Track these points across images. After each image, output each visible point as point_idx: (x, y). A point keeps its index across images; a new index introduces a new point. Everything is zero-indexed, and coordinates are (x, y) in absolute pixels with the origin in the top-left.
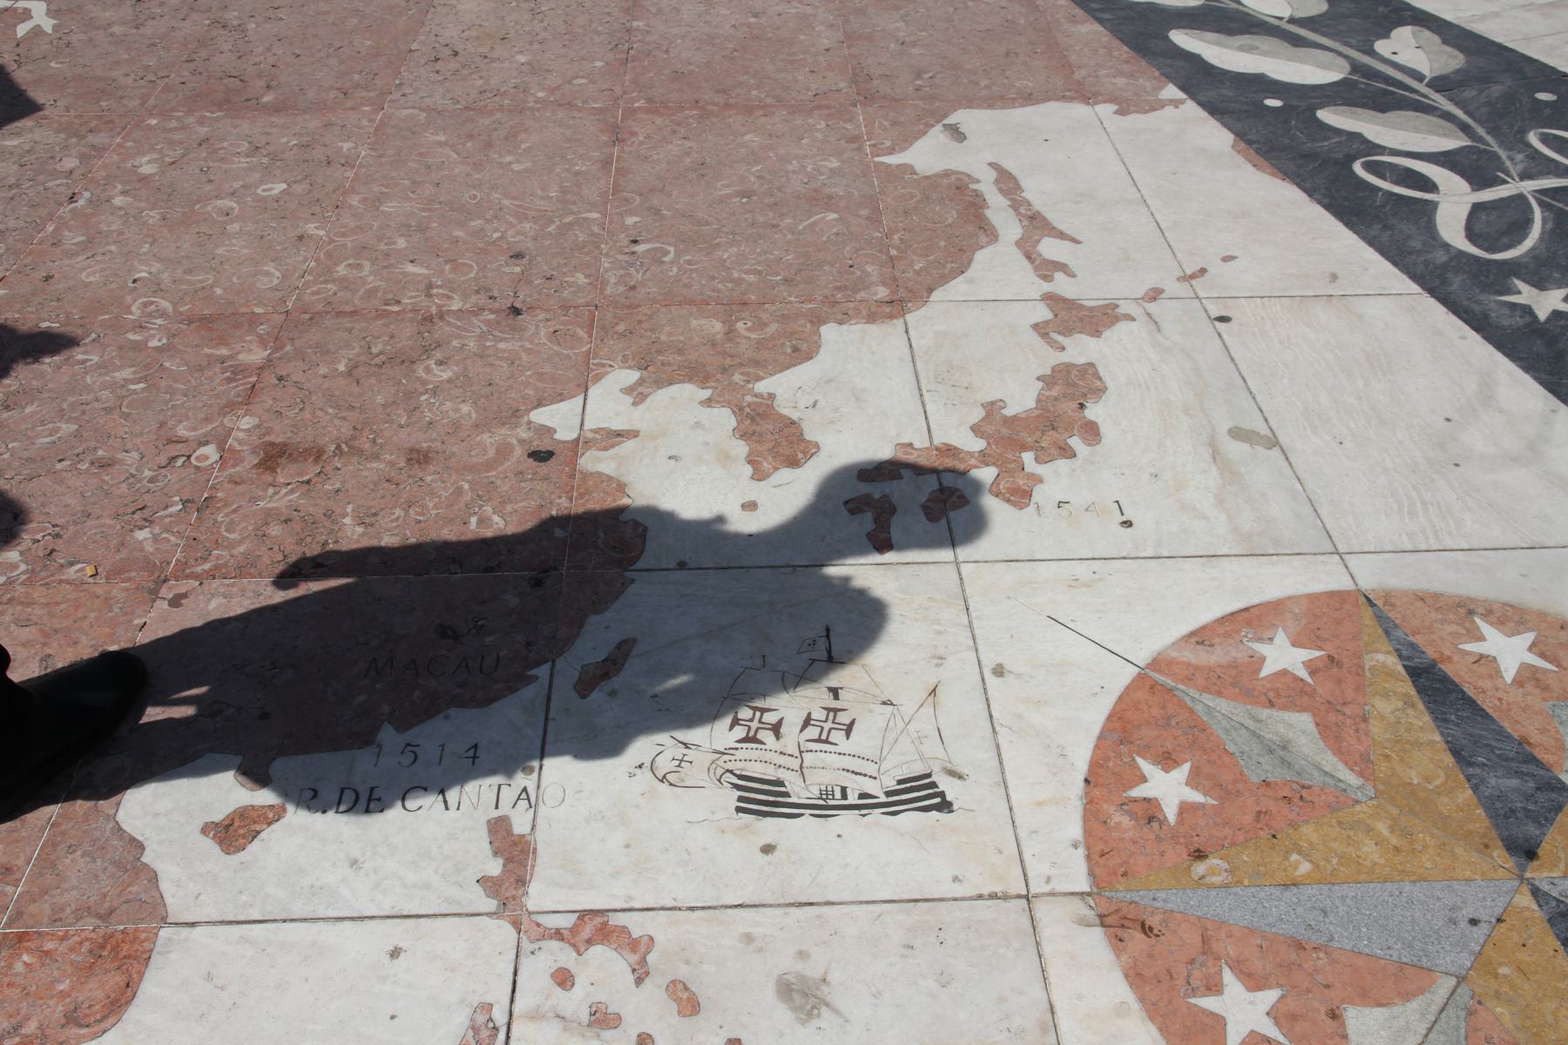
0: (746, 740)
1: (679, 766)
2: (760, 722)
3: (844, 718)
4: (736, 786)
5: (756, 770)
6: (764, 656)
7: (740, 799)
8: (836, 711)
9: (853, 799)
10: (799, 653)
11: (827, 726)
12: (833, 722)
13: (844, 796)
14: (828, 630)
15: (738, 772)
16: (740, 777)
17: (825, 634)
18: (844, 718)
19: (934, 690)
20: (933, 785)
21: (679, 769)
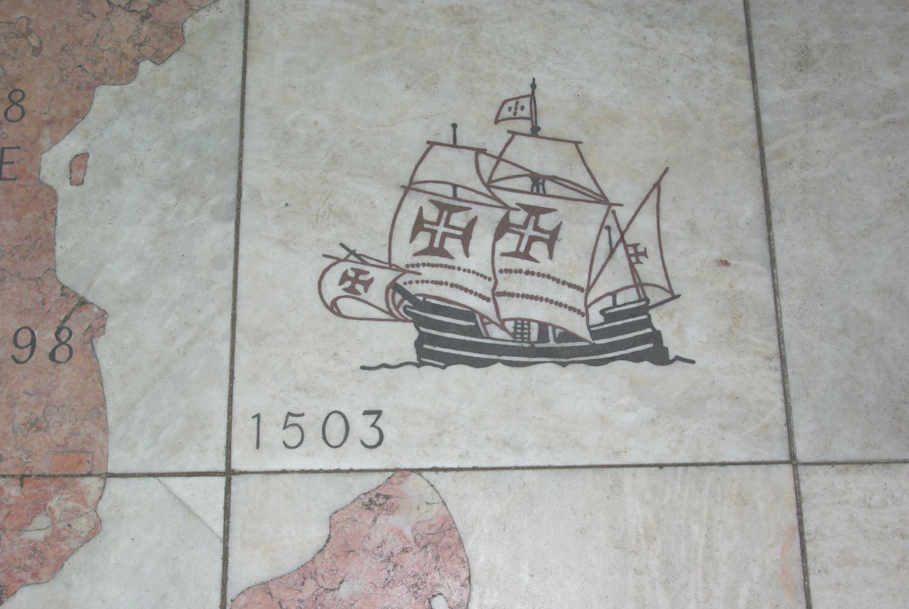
0: (430, 251)
3: (547, 222)
4: (418, 322)
6: (454, 126)
9: (552, 343)
10: (497, 121)
14: (533, 86)
15: (421, 298)
17: (529, 92)
19: (657, 185)
20: (648, 323)
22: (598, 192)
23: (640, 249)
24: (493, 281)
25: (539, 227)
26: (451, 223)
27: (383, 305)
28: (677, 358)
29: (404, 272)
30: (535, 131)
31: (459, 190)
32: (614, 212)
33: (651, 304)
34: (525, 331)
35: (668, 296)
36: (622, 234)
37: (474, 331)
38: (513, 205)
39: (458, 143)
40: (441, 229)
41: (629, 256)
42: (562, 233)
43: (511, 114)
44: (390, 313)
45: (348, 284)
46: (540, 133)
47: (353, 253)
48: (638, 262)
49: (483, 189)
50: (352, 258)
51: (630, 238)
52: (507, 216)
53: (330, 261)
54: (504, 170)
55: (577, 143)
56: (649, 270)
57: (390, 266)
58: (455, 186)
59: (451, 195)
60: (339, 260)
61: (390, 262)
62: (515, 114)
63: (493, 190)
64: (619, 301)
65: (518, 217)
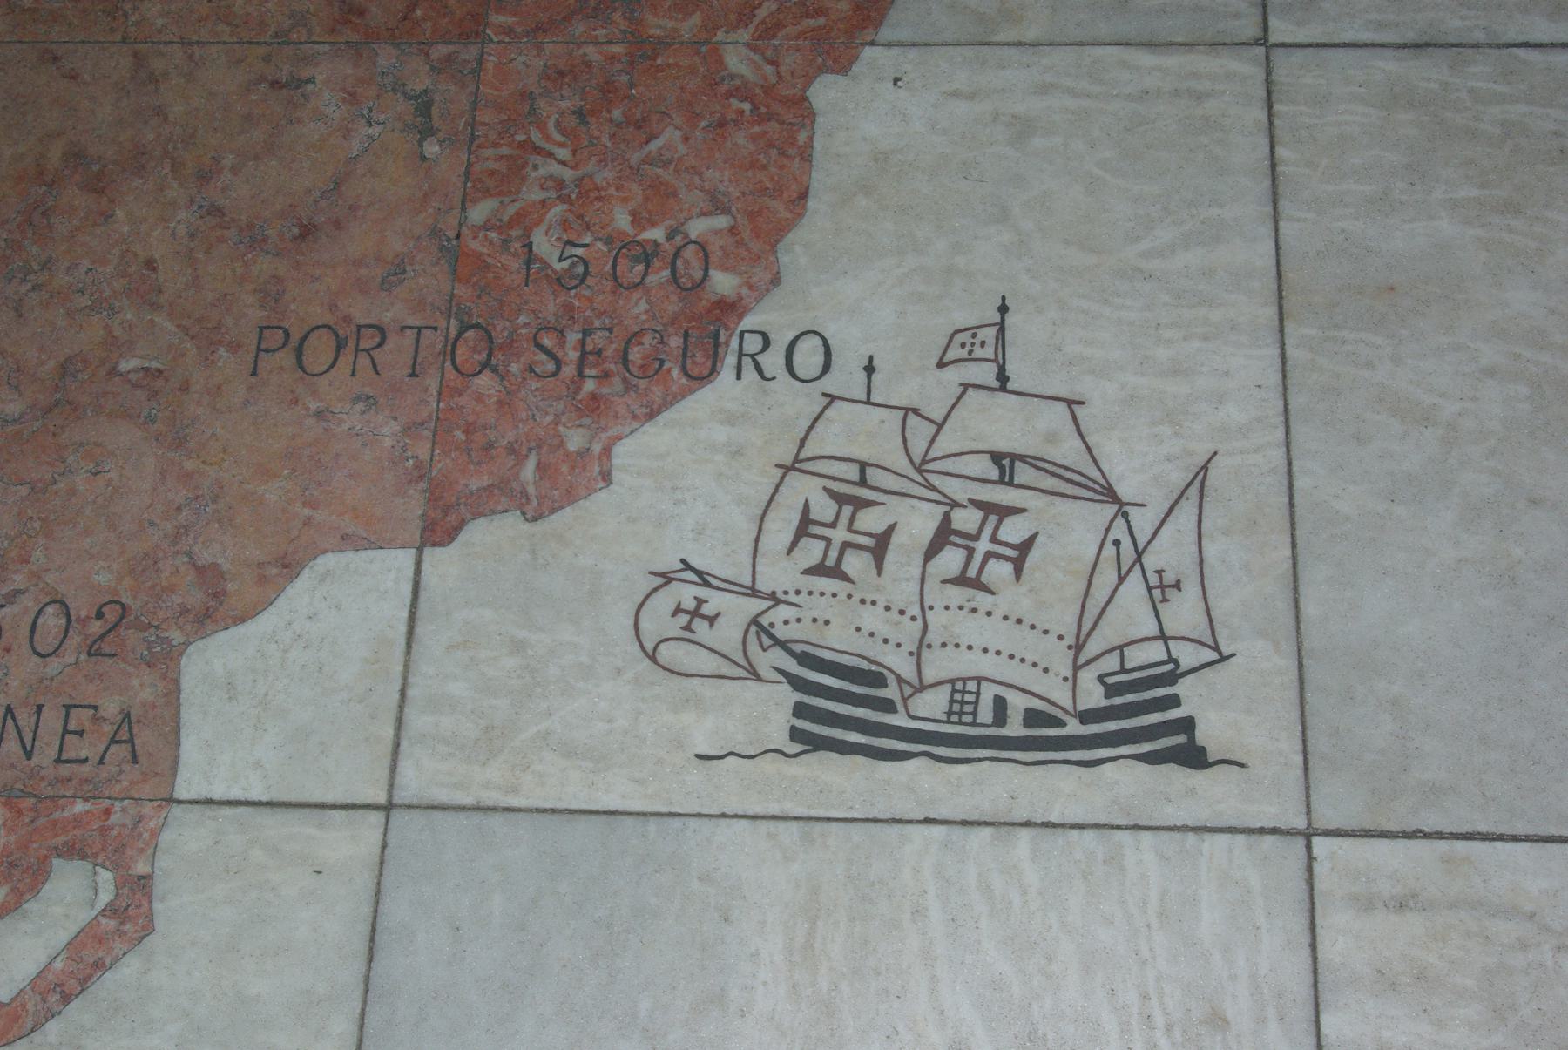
0: (818, 570)
1: (687, 628)
3: (1013, 531)
4: (797, 683)
5: (839, 641)
7: (800, 710)
8: (1005, 512)
9: (1015, 728)
10: (941, 365)
12: (994, 539)
14: (1003, 309)
15: (798, 648)
16: (805, 659)
18: (1013, 531)
21: (687, 635)
22: (1105, 484)
23: (1169, 578)
24: (919, 622)
25: (997, 539)
30: (1003, 377)
31: (869, 471)
32: (1125, 515)
33: (1183, 668)
36: (1139, 555)
37: (888, 706)
38: (960, 497)
39: (875, 398)
43: (964, 353)
45: (684, 619)
46: (1010, 386)
48: (1165, 600)
51: (1150, 561)
52: (947, 518)
55: (1070, 403)
56: (1183, 613)
57: (753, 592)
58: (863, 466)
59: (855, 477)
61: (752, 588)
62: (970, 352)
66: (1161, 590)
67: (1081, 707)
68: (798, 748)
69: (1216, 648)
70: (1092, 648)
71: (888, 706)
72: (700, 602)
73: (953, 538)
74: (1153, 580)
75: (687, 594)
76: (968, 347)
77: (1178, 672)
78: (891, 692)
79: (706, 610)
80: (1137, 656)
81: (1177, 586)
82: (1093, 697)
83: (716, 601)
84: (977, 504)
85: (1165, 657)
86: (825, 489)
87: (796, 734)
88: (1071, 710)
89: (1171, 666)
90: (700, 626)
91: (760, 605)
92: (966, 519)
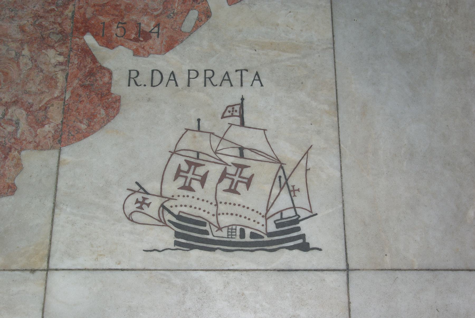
1: (141, 208)
2: (193, 174)
3: (247, 173)
6: (199, 120)
7: (177, 235)
8: (243, 167)
9: (248, 239)
10: (223, 117)
11: (236, 178)
13: (242, 234)
14: (243, 99)
18: (247, 173)
19: (307, 152)
20: (299, 229)
23: (296, 188)
26: (195, 173)
27: (157, 217)
28: (313, 249)
29: (169, 199)
31: (200, 154)
34: (233, 231)
35: (310, 214)
36: (287, 180)
39: (201, 129)
40: (190, 175)
41: (290, 191)
42: (254, 180)
44: (160, 221)
45: (138, 205)
47: (141, 187)
48: (295, 196)
49: (214, 155)
50: (141, 191)
51: (291, 182)
52: (225, 169)
53: (130, 192)
54: (224, 143)
55: (264, 130)
56: (301, 200)
57: (161, 196)
58: (198, 153)
59: (196, 156)
60: (134, 192)
63: (218, 155)
64: (284, 216)
65: (232, 170)
66: (292, 192)
67: (269, 231)
68: (177, 247)
69: (311, 212)
70: (272, 211)
71: (206, 233)
72: (144, 199)
73: (227, 176)
74: (291, 188)
75: (139, 196)
76: (231, 112)
77: (300, 219)
78: (207, 228)
79: (147, 202)
80: (286, 214)
81: (298, 190)
82: (272, 228)
83: (151, 199)
84: (235, 164)
85: (294, 214)
86: (185, 160)
87: (176, 243)
88: (265, 232)
89: (297, 217)
90: (144, 206)
91: (164, 200)
92: (232, 170)
